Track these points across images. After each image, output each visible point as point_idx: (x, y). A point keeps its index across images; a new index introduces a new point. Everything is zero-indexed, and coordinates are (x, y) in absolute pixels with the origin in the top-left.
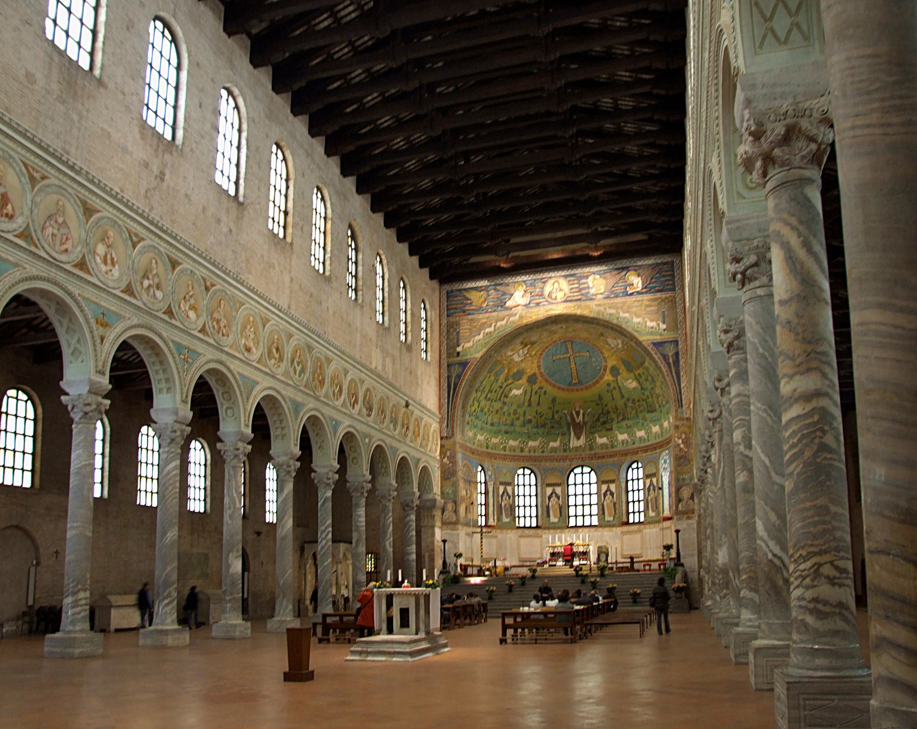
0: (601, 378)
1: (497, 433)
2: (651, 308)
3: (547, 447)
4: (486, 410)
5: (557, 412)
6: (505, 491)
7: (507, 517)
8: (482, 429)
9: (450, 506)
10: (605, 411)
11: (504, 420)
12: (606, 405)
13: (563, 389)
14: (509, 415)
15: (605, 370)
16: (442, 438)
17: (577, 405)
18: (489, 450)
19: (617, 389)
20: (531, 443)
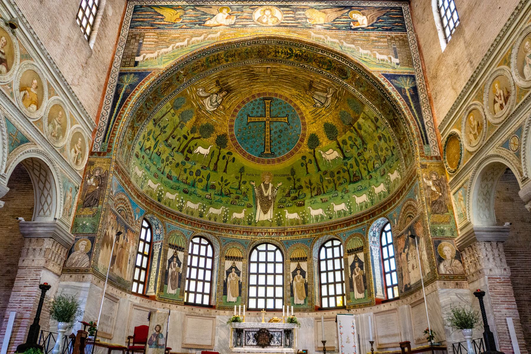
0: (296, 150)
1: (174, 189)
2: (380, 44)
3: (230, 218)
4: (164, 157)
5: (244, 183)
6: (175, 256)
7: (173, 289)
8: (156, 176)
9: (83, 245)
10: (296, 187)
12: (299, 180)
13: (253, 159)
14: (191, 173)
15: (302, 140)
16: (92, 154)
18: (162, 204)
19: (313, 161)
20: (212, 210)
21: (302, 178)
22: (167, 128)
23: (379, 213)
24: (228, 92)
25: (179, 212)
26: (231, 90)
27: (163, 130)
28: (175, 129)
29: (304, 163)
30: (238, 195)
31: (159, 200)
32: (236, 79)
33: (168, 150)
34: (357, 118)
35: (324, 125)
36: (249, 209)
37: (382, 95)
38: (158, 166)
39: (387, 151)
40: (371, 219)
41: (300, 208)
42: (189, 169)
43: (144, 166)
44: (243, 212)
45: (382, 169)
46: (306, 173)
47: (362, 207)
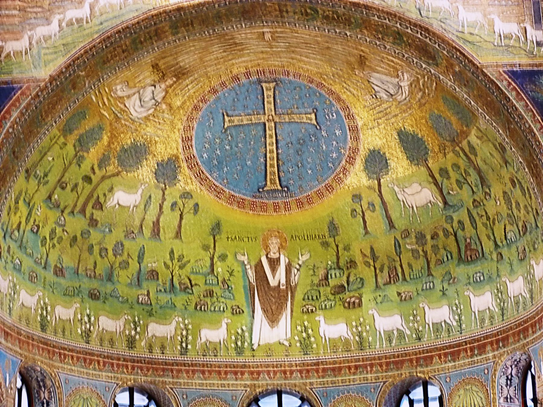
4: (46, 232)
8: (33, 278)
10: (342, 263)
11: (91, 266)
12: (347, 248)
13: (241, 204)
15: (351, 160)
17: (274, 244)
18: (49, 336)
21: (354, 244)
22: (50, 175)
23: (515, 342)
24: (178, 78)
25: (83, 345)
26: (184, 74)
27: (42, 180)
28: (65, 170)
29: (359, 210)
30: (211, 287)
31: (43, 328)
32: (195, 54)
33: (53, 215)
34: (465, 134)
35: (399, 135)
36: (235, 317)
37: (506, 113)
38: (35, 255)
39: (528, 213)
40: (501, 351)
41: (353, 314)
42: (100, 243)
43: (10, 266)
44: (224, 326)
45: (520, 244)
46: (362, 231)
47: (483, 321)
